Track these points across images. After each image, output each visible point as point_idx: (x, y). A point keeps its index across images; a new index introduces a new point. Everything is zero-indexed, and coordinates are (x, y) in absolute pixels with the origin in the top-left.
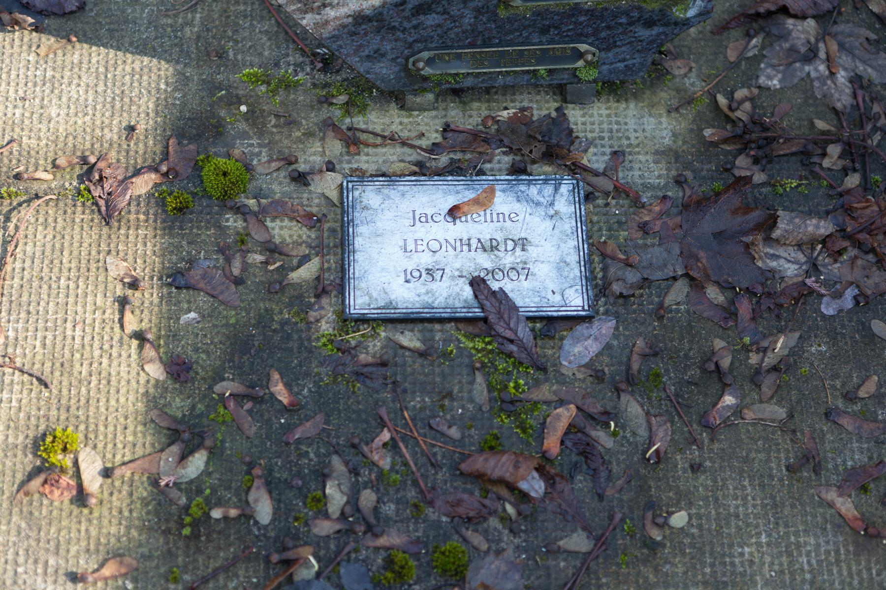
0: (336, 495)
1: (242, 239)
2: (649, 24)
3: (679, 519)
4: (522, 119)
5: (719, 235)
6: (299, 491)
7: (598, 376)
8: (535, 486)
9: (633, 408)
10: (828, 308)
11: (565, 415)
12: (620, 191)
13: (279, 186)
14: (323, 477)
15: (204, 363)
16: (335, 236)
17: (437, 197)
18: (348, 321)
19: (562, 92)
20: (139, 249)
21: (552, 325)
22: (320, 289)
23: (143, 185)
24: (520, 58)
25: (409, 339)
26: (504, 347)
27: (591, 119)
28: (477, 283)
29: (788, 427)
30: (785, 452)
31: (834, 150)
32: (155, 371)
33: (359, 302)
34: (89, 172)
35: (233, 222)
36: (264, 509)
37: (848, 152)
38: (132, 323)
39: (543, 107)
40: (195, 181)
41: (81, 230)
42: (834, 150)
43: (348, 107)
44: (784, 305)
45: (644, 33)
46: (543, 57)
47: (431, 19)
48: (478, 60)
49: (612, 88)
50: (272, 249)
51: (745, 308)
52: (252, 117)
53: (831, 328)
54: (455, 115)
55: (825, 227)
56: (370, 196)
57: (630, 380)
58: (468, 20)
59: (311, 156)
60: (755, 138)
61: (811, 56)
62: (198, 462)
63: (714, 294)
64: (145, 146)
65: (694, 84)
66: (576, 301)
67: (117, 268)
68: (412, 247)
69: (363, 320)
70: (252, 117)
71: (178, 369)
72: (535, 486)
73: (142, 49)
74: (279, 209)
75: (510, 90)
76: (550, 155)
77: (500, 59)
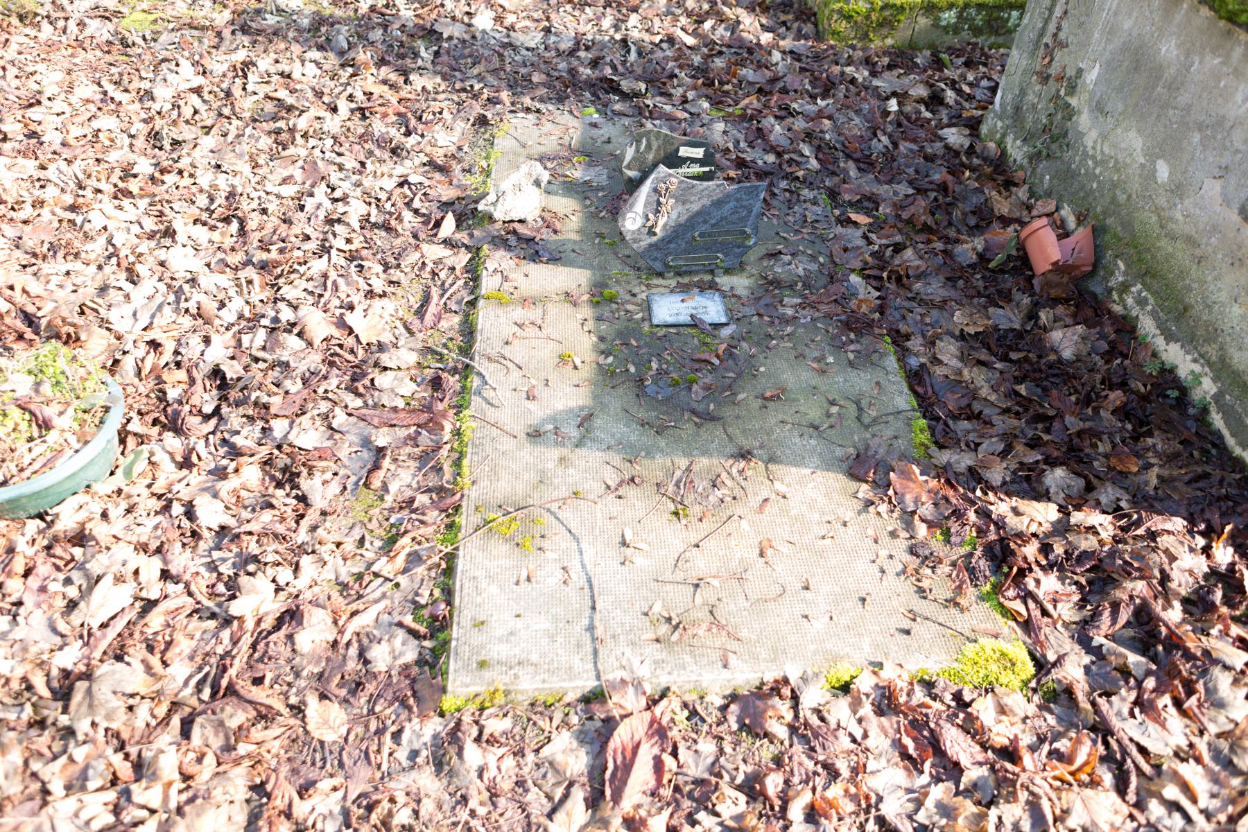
0: (654, 365)
1: (618, 310)
2: (739, 247)
3: (762, 369)
4: (701, 281)
5: (766, 305)
6: (643, 365)
7: (733, 338)
8: (716, 362)
9: (744, 345)
10: (803, 321)
11: (724, 346)
12: (734, 296)
13: (628, 297)
14: (650, 361)
15: (609, 337)
16: (647, 307)
17: (678, 297)
18: (652, 326)
19: (712, 272)
20: (586, 312)
21: (716, 326)
22: (643, 319)
23: (586, 297)
24: (699, 259)
25: (673, 330)
26: (703, 331)
27: (724, 281)
28: (692, 316)
29: (794, 348)
30: (794, 353)
31: (800, 284)
32: (595, 339)
33: (655, 321)
34: (567, 294)
35: (614, 306)
36: (632, 369)
37: (804, 285)
38: (586, 329)
39: (708, 278)
40: (600, 297)
41: (568, 308)
42: (800, 284)
43: (647, 279)
44: (787, 321)
45: (738, 251)
46: (707, 258)
47: (672, 246)
48: (687, 259)
49: (728, 271)
50: (627, 311)
51: (777, 321)
52: (617, 282)
53: (804, 325)
54: (680, 280)
55: (799, 301)
56: (656, 298)
57: (743, 339)
58: (683, 246)
59: (636, 290)
60: (776, 283)
61: (790, 264)
62: (610, 359)
63: (766, 318)
64: (585, 288)
65: (754, 271)
66: (724, 320)
67: (580, 316)
68: (669, 308)
69: (658, 326)
70: (617, 282)
71: (602, 339)
72: (716, 362)
73: (581, 267)
74: (628, 302)
75: (697, 273)
76: (710, 288)
77: (694, 259)
